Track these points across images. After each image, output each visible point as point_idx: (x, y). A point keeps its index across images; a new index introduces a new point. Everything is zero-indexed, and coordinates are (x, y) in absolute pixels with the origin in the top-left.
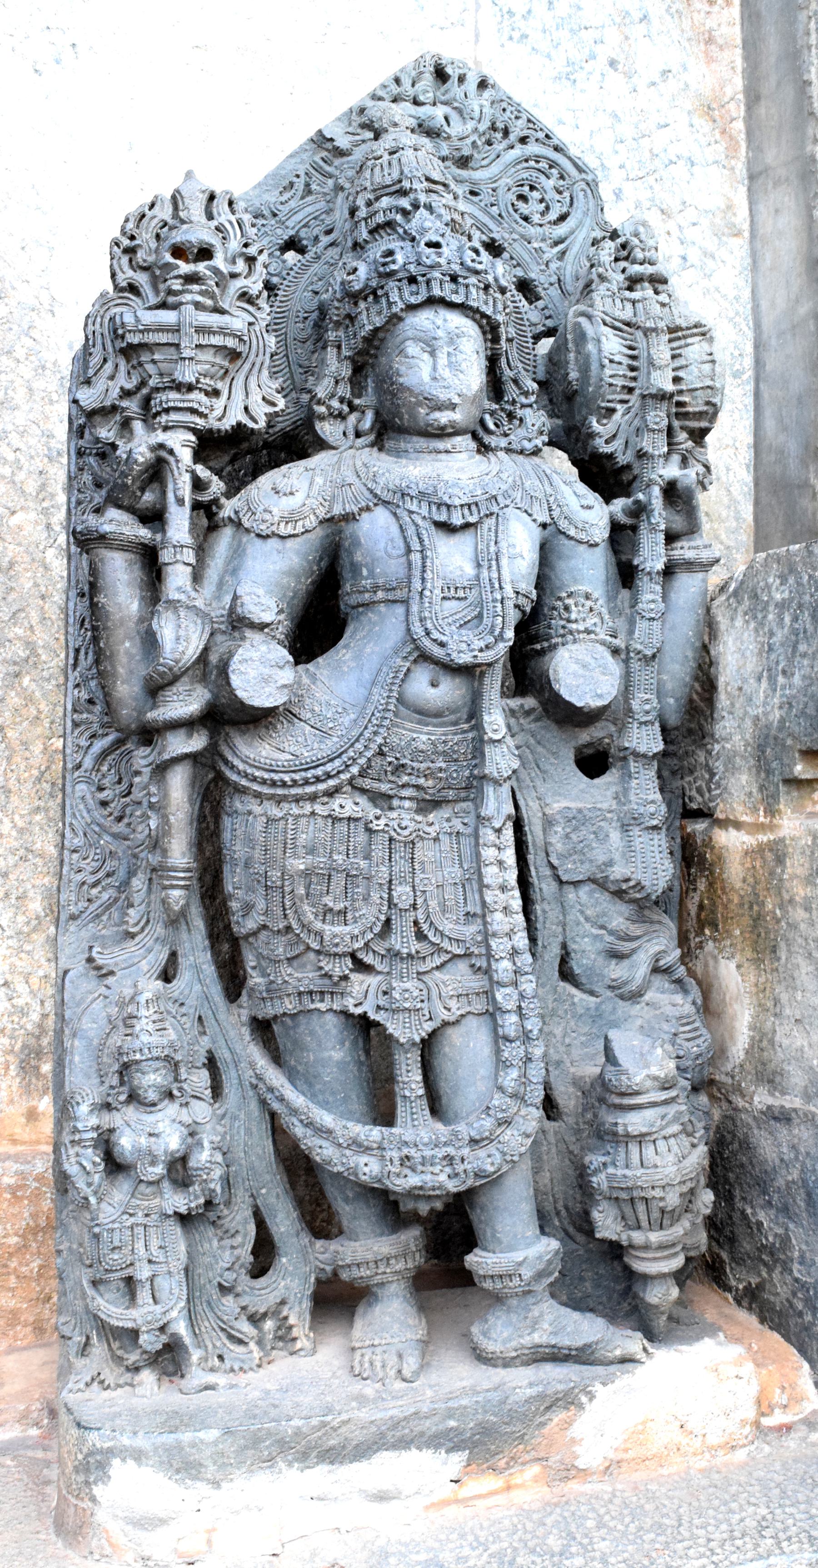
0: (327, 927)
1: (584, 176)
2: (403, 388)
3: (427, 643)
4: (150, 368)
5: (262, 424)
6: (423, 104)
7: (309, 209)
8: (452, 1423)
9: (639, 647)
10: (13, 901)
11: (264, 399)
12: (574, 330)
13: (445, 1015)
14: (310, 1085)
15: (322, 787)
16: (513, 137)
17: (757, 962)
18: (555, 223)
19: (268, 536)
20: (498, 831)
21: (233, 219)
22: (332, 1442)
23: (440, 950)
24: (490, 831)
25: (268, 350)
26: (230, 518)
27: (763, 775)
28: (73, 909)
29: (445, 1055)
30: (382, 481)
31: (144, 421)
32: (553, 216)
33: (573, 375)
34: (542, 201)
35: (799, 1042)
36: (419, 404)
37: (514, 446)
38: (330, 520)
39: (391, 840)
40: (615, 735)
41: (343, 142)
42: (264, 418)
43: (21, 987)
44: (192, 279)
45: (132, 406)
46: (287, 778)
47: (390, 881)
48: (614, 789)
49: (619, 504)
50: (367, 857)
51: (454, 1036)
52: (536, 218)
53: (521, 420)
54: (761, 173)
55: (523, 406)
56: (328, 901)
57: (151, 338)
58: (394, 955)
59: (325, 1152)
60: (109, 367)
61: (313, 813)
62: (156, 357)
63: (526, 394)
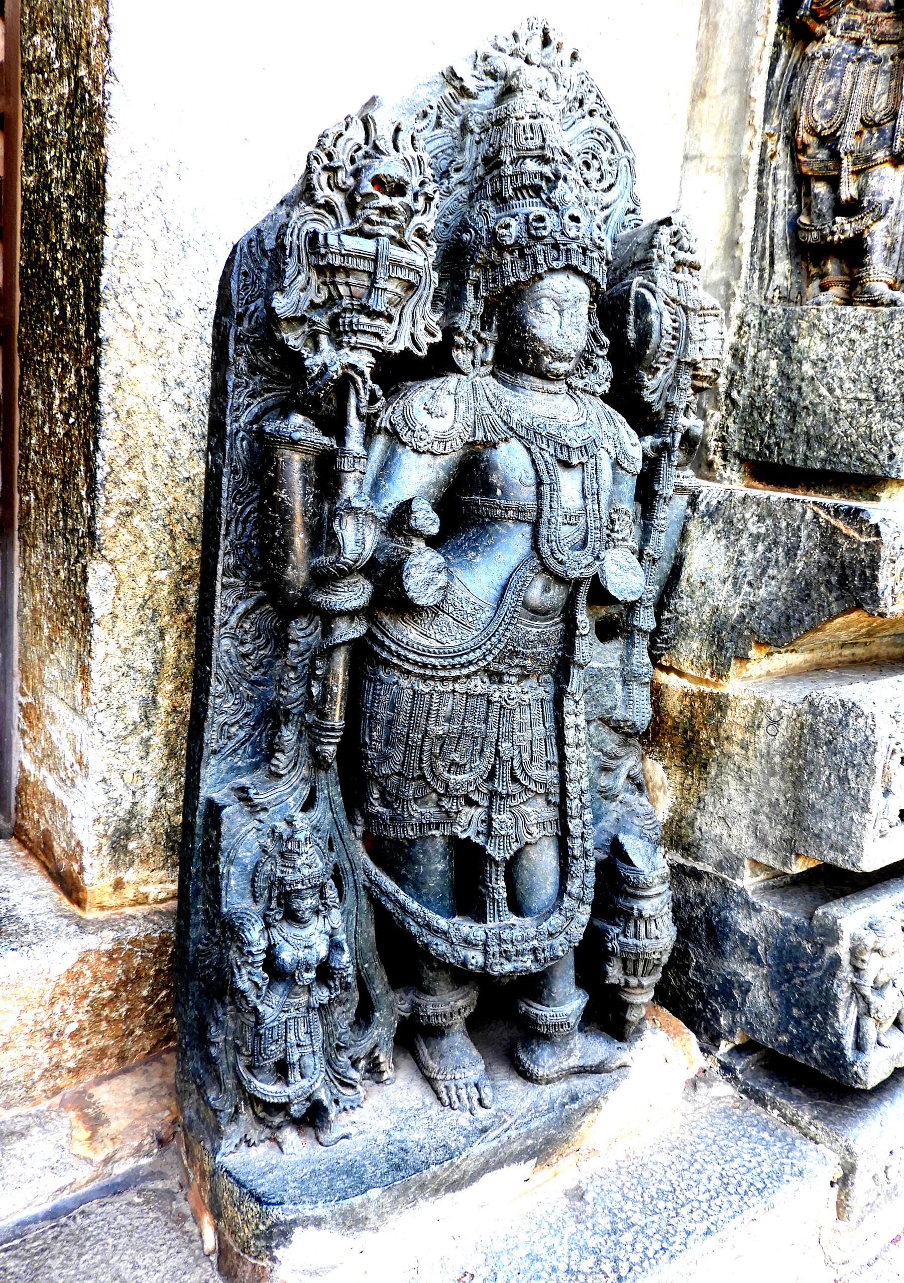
0: (452, 777)
1: (627, 153)
2: (535, 338)
3: (552, 562)
4: (343, 290)
5: (424, 353)
6: (532, 64)
7: (439, 142)
8: (530, 1142)
9: (651, 552)
10: (114, 711)
11: (426, 329)
12: (636, 298)
13: (528, 838)
14: (417, 889)
15: (465, 671)
16: (586, 108)
17: (686, 770)
18: (604, 191)
19: (424, 452)
20: (577, 702)
21: (415, 154)
22: (456, 1177)
23: (527, 790)
24: (572, 703)
25: (433, 286)
26: (386, 428)
27: (715, 648)
28: (214, 746)
29: (522, 865)
30: (515, 416)
31: (329, 335)
32: (605, 184)
33: (632, 335)
34: (599, 169)
35: (717, 831)
36: (546, 353)
37: (588, 388)
38: (474, 443)
39: (502, 707)
40: (625, 613)
41: (471, 84)
42: (426, 347)
43: (116, 781)
44: (388, 211)
45: (322, 320)
46: (436, 662)
47: (497, 741)
48: (619, 652)
49: (649, 440)
50: (486, 721)
51: (532, 852)
52: (594, 185)
53: (595, 368)
54: (695, 157)
55: (598, 356)
56: (455, 757)
57: (351, 263)
58: (493, 795)
59: (440, 948)
60: (302, 278)
61: (454, 691)
62: (351, 280)
63: (602, 347)
